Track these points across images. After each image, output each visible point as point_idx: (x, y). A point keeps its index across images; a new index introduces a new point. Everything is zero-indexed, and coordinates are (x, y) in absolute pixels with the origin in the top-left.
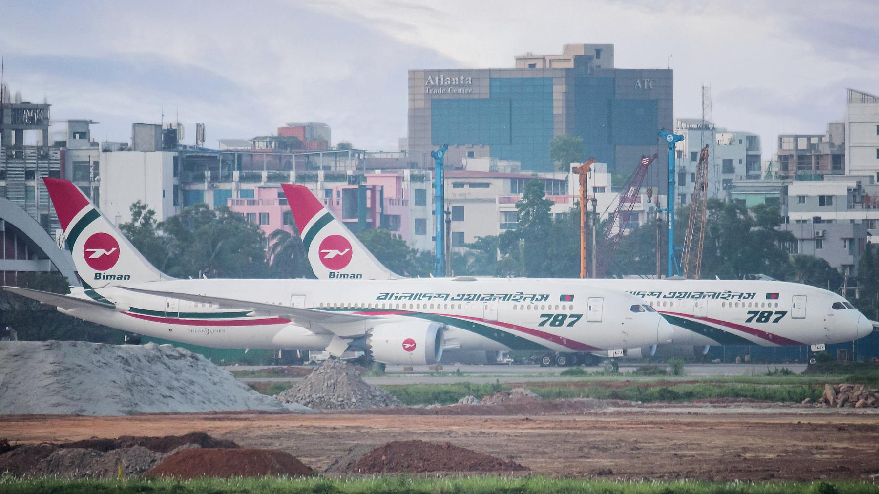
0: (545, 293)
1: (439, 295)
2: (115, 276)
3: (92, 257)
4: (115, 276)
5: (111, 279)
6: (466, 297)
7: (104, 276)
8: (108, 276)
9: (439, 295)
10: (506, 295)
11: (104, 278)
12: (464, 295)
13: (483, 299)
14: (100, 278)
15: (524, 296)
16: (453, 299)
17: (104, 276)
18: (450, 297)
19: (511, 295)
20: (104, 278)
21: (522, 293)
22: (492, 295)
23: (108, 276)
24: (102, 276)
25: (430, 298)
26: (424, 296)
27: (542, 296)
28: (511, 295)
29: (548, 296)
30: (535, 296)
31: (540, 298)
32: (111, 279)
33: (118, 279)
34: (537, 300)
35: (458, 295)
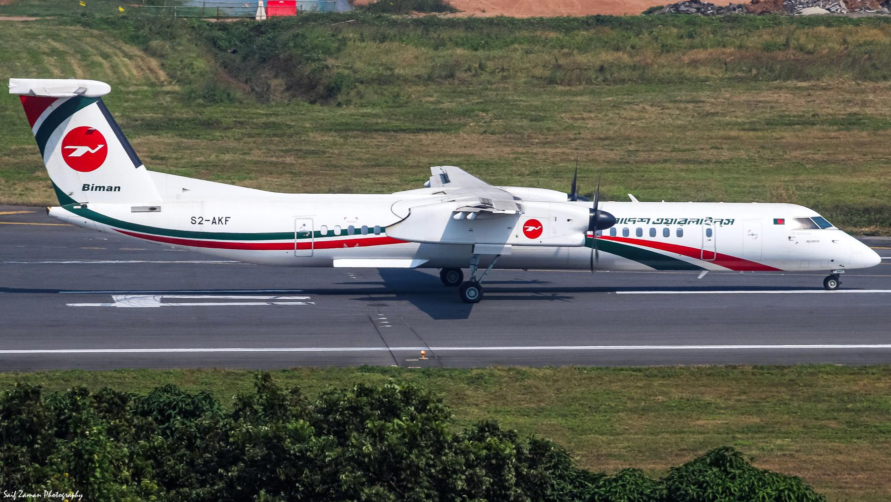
0: (731, 218)
1: (642, 220)
2: (104, 187)
3: (73, 155)
4: (104, 187)
5: (100, 190)
6: (664, 221)
7: (93, 187)
8: (97, 187)
9: (642, 220)
10: (699, 220)
11: (92, 190)
12: (662, 220)
13: (679, 223)
14: (88, 189)
15: (714, 221)
16: (654, 223)
17: (93, 187)
18: (651, 222)
19: (702, 220)
20: (92, 190)
21: (711, 218)
22: (686, 220)
23: (97, 187)
24: (90, 187)
25: (634, 222)
26: (629, 221)
27: (728, 220)
28: (702, 220)
29: (733, 220)
30: (722, 220)
31: (727, 222)
32: (100, 190)
33: (107, 190)
34: (725, 224)
35: (658, 220)
